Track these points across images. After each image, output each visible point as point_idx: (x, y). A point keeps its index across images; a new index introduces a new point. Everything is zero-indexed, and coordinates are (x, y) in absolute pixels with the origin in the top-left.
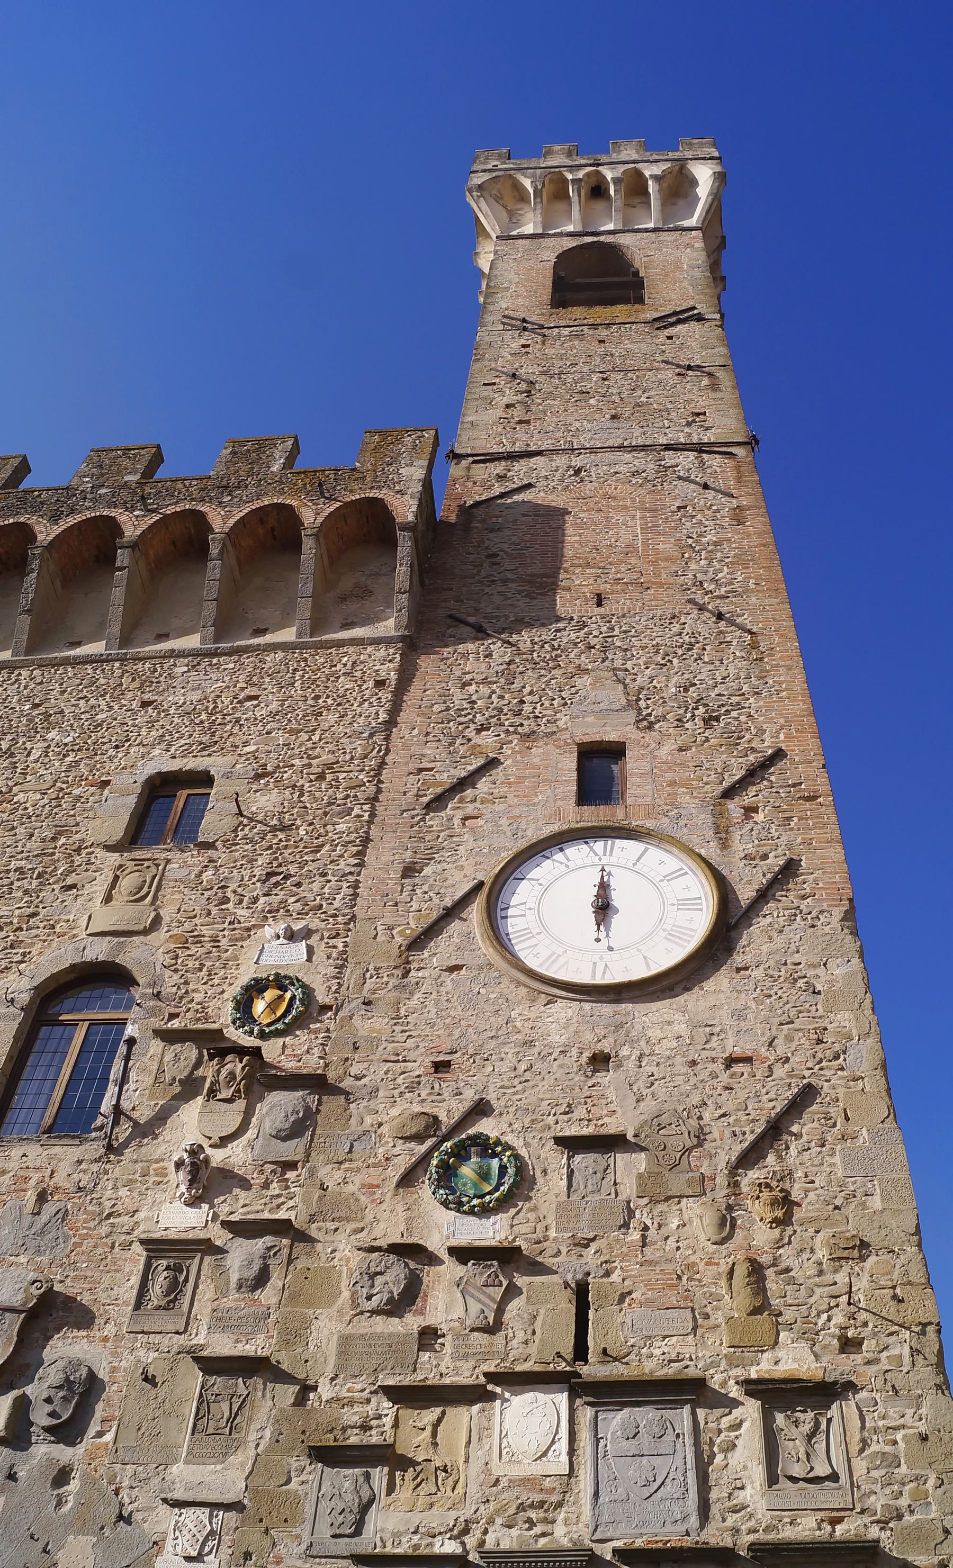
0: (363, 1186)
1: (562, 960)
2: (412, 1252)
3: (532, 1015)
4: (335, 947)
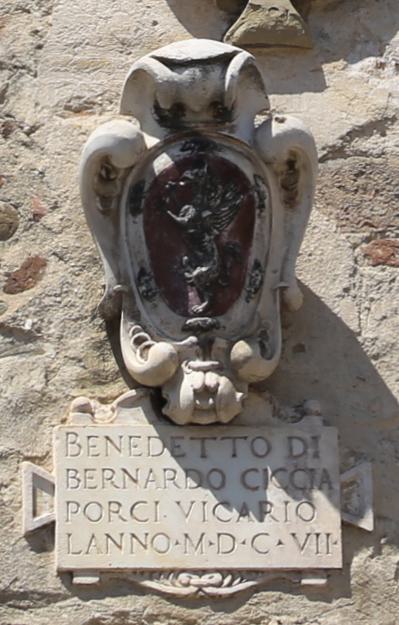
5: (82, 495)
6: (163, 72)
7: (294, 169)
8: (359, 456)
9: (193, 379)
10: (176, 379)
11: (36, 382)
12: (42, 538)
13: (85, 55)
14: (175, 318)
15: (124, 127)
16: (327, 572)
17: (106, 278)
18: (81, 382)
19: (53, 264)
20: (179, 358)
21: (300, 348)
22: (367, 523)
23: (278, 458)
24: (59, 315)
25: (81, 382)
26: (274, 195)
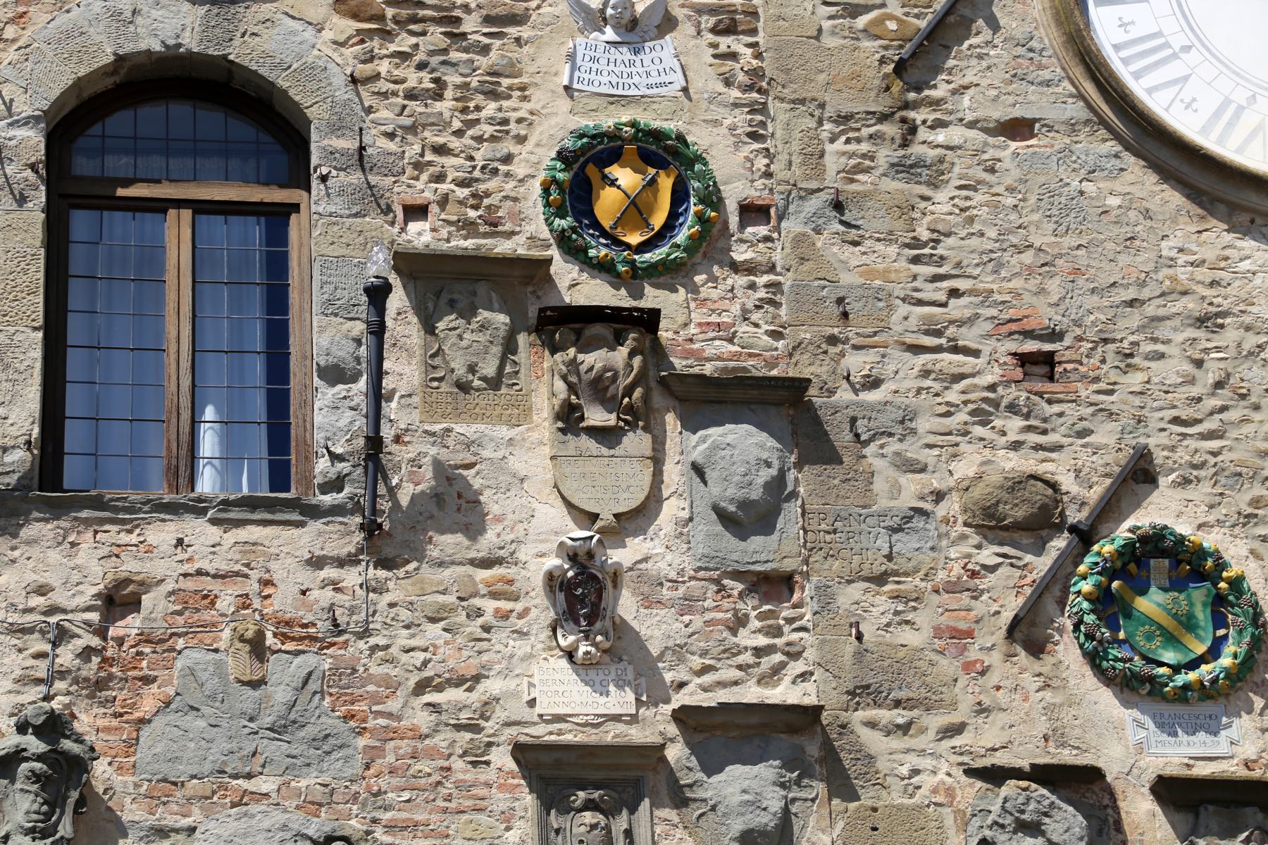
0: (938, 632)
1: (1249, 120)
2: (1079, 783)
3: (1210, 254)
4: (733, 56)
5: (546, 689)
6: (570, 542)
7: (616, 576)
8: (641, 676)
10: (577, 649)
11: (529, 649)
12: (532, 703)
13: (542, 537)
14: (576, 628)
15: (558, 562)
16: (631, 715)
17: (552, 614)
18: (544, 650)
19: (533, 609)
20: (578, 641)
22: (644, 698)
23: (613, 675)
24: (536, 627)
25: (544, 650)
26: (609, 584)
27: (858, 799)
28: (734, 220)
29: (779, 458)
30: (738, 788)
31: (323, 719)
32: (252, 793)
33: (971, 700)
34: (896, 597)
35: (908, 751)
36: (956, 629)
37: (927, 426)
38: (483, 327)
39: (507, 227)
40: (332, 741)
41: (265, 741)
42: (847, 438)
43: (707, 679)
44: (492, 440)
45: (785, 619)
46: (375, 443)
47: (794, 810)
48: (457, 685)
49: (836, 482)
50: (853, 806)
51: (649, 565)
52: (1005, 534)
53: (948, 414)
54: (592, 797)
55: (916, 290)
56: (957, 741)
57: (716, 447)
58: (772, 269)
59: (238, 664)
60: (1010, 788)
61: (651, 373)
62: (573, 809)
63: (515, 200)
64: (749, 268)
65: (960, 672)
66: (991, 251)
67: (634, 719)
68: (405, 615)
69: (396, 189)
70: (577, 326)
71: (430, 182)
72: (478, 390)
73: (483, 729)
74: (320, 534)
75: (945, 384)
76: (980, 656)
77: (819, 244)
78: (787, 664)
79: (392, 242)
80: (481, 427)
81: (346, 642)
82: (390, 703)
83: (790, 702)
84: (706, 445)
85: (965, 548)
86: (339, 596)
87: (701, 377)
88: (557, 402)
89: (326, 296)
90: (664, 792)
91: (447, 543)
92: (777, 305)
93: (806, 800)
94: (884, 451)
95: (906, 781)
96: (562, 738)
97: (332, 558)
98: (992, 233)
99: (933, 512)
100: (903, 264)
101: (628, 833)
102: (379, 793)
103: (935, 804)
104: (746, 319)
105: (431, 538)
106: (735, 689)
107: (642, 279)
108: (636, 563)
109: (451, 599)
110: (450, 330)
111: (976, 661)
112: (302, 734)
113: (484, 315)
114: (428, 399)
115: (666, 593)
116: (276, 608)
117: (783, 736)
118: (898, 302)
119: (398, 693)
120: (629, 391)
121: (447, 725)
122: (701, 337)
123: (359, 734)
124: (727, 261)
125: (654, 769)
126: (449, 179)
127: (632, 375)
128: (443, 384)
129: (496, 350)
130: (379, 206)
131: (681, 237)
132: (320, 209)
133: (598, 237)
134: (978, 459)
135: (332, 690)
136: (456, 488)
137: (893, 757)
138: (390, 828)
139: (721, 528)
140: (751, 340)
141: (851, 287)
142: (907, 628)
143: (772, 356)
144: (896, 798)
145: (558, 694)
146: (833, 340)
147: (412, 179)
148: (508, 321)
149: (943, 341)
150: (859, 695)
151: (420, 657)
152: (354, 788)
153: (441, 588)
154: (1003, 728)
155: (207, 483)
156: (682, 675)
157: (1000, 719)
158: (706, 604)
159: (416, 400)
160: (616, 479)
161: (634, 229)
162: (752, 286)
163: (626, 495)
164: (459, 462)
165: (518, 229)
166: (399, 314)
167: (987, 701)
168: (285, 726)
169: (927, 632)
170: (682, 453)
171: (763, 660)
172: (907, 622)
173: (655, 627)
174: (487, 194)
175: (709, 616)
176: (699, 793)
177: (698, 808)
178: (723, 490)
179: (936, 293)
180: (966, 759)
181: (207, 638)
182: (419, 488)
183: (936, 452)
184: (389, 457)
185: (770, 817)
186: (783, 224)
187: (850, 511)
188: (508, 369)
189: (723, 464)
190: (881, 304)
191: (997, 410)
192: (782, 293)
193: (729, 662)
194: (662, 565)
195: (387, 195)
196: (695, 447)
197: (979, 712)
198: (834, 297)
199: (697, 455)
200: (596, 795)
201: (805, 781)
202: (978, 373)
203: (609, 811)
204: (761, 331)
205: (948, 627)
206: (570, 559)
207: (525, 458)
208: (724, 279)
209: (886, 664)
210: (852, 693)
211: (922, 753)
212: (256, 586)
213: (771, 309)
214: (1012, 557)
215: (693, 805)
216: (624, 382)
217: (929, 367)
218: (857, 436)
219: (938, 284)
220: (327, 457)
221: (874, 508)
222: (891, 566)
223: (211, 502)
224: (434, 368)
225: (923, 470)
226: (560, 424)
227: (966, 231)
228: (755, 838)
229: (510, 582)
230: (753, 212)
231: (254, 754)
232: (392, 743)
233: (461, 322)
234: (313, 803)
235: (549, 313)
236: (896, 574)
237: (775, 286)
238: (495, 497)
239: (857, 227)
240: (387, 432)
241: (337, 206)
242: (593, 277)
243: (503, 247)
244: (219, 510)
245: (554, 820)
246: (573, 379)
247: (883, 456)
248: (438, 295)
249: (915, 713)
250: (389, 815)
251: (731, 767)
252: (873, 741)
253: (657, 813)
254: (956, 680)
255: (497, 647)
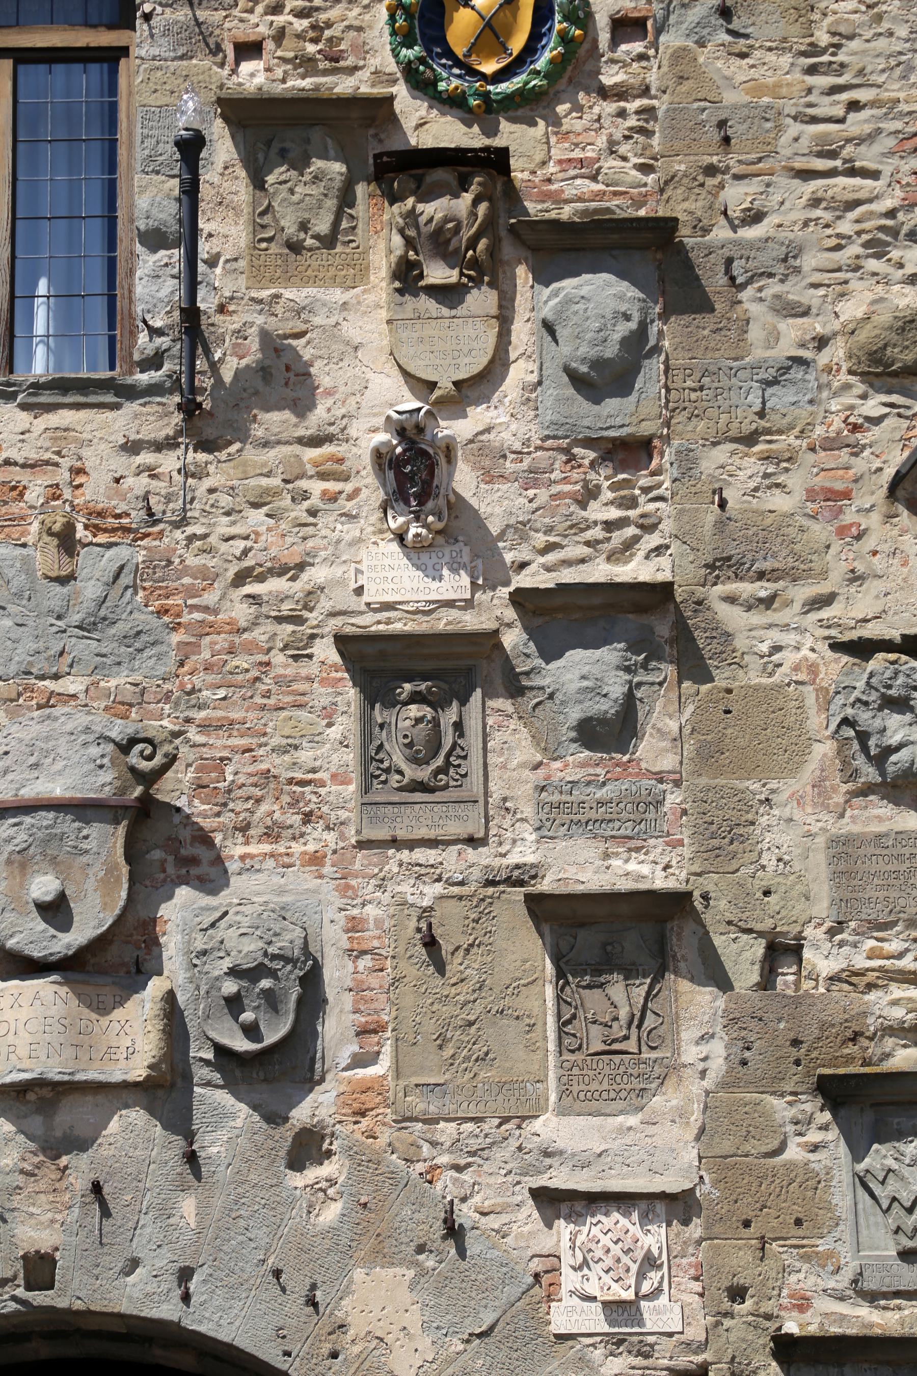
0: (811, 495)
5: (373, 575)
6: (395, 416)
7: (449, 451)
8: (478, 557)
9: (413, 530)
11: (358, 534)
12: (359, 591)
14: (406, 508)
16: (465, 600)
17: (381, 495)
18: (374, 533)
20: (408, 523)
21: (457, 517)
22: (480, 582)
23: (447, 558)
25: (374, 533)
26: (442, 460)
27: (712, 680)
28: (604, 38)
29: (641, 309)
30: (577, 674)
31: (136, 615)
32: (59, 694)
33: (844, 567)
34: (766, 458)
35: (770, 626)
36: (831, 490)
37: (813, 263)
38: (316, 179)
39: (350, 62)
40: (144, 638)
41: (74, 640)
42: (721, 282)
43: (552, 558)
44: (324, 305)
45: (641, 488)
46: (191, 315)
47: (638, 694)
48: (280, 575)
49: (706, 332)
50: (705, 688)
51: (491, 436)
52: (894, 381)
53: (838, 248)
54: (418, 689)
55: (810, 105)
56: (825, 613)
57: (569, 301)
58: (645, 91)
59: (46, 558)
60: (878, 662)
61: (501, 221)
62: (398, 702)
63: (360, 29)
64: (620, 93)
65: (834, 537)
66: (901, 53)
67: (469, 604)
68: (225, 501)
69: (227, 25)
70: (420, 171)
71: (266, 14)
72: (310, 250)
73: (306, 620)
74: (136, 416)
75: (838, 213)
76: (856, 518)
77: (701, 60)
78: (641, 537)
79: (221, 86)
80: (312, 291)
81: (161, 532)
82: (206, 596)
83: (641, 579)
84: (557, 300)
85: (849, 399)
86: (154, 483)
87: (555, 223)
88: (393, 259)
89: (147, 152)
90: (498, 680)
91: (274, 421)
92: (648, 133)
93: (652, 684)
94: (763, 295)
95: (766, 659)
96: (391, 627)
97: (148, 442)
98: (902, 31)
99: (814, 361)
100: (797, 75)
101: (459, 726)
102: (193, 691)
103: (796, 682)
104: (612, 152)
105: (255, 416)
106: (582, 567)
107: (498, 112)
108: (477, 434)
109: (275, 482)
110: (280, 183)
111: (851, 525)
112: (112, 631)
113: (318, 164)
114: (256, 262)
115: (509, 466)
116: (88, 498)
117: (630, 616)
118: (789, 121)
119: (216, 585)
120: (473, 243)
121: (268, 617)
122: (561, 176)
123: (174, 629)
124: (595, 85)
125: (488, 657)
126: (287, 10)
127: (476, 225)
128: (273, 245)
129: (331, 204)
130: (207, 45)
131: (542, 62)
132: (143, 53)
133: (451, 67)
134: (870, 296)
135: (146, 584)
136: (285, 360)
137: (753, 633)
138: (204, 727)
139: (572, 391)
140: (616, 176)
141: (735, 107)
142: (777, 491)
143: (640, 194)
144: (755, 678)
145: (384, 577)
146: (711, 171)
147: (246, 11)
148: (344, 169)
149: (838, 163)
150: (719, 568)
151: (241, 544)
152: (167, 686)
153: (265, 470)
154: (877, 597)
155: (39, 364)
156: (524, 554)
157: (875, 586)
158: (553, 476)
159: (242, 264)
160: (457, 341)
161: (490, 55)
162: (622, 114)
163: (467, 360)
164: (288, 331)
165: (361, 63)
166: (226, 168)
167: (861, 568)
168: (94, 624)
169: (799, 495)
170: (533, 309)
171: (614, 535)
172: (778, 485)
173: (495, 504)
174: (329, 25)
175: (555, 489)
176: (537, 681)
177: (535, 697)
178: (575, 349)
179: (833, 106)
180: (833, 632)
181: (15, 532)
182: (244, 362)
183: (822, 292)
184: (212, 329)
185: (611, 703)
186: (662, 39)
187: (719, 365)
188: (344, 224)
189: (575, 319)
190: (768, 125)
191: (896, 239)
192: (656, 119)
193: (577, 538)
194: (506, 435)
195: (217, 32)
196: (546, 302)
197: (852, 581)
198: (714, 121)
199: (547, 312)
200: (423, 686)
201: (653, 664)
202: (877, 197)
203: (438, 703)
204: (630, 165)
205: (822, 488)
206: (399, 434)
207: (360, 324)
208: (591, 107)
209: (751, 533)
210: (711, 567)
211: (785, 628)
212: (67, 475)
213: (641, 139)
214: (900, 407)
215: (530, 694)
216: (467, 233)
217: (820, 194)
218: (733, 279)
219: (837, 97)
220: (146, 332)
221: (747, 359)
222: (763, 423)
223: (20, 385)
224: (263, 227)
225: (806, 313)
226: (397, 284)
227: (872, 32)
228: (595, 726)
229: (341, 461)
230: (626, 26)
231: (61, 654)
232: (208, 638)
233: (293, 173)
234: (123, 703)
235: (385, 159)
236: (769, 432)
237: (648, 112)
238: (327, 369)
239: (746, 36)
240: (206, 302)
241: (162, 48)
242: (443, 114)
243: (344, 86)
244: (29, 394)
245: (379, 714)
246: (412, 233)
247: (761, 300)
248: (269, 144)
249: (781, 583)
250: (203, 714)
251: (572, 652)
252: (732, 617)
253: (490, 703)
254: (828, 547)
255: (324, 532)
